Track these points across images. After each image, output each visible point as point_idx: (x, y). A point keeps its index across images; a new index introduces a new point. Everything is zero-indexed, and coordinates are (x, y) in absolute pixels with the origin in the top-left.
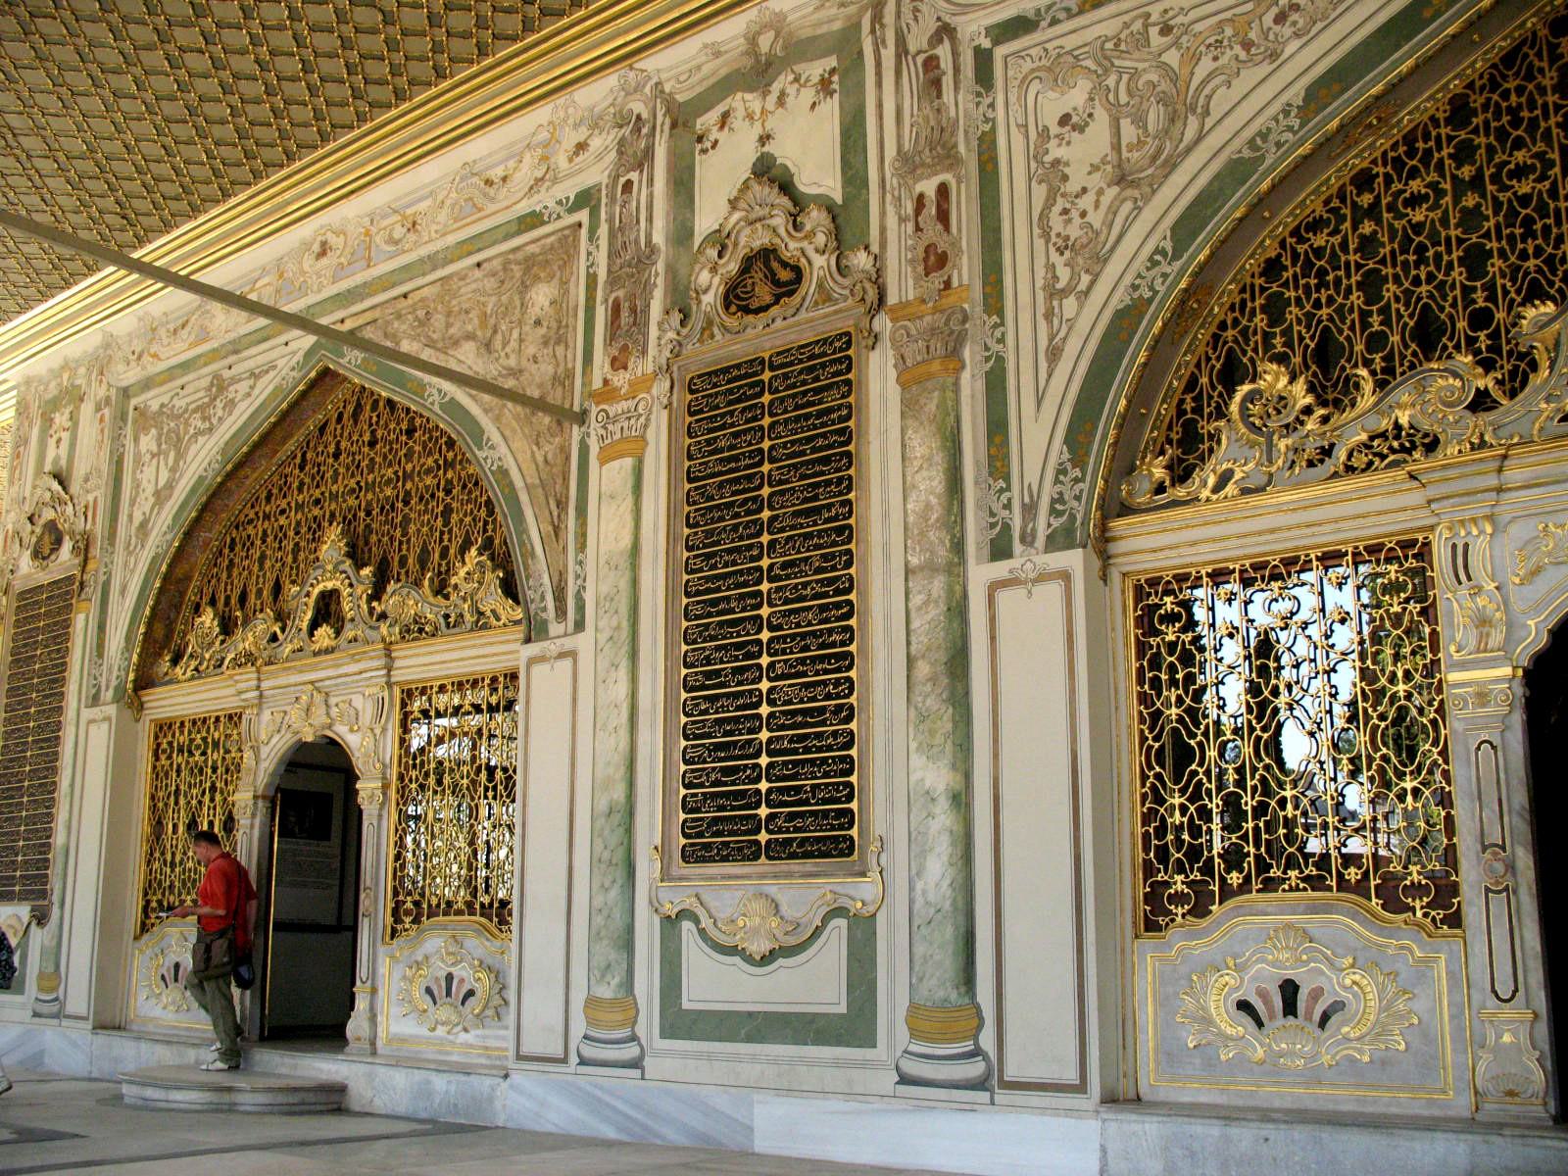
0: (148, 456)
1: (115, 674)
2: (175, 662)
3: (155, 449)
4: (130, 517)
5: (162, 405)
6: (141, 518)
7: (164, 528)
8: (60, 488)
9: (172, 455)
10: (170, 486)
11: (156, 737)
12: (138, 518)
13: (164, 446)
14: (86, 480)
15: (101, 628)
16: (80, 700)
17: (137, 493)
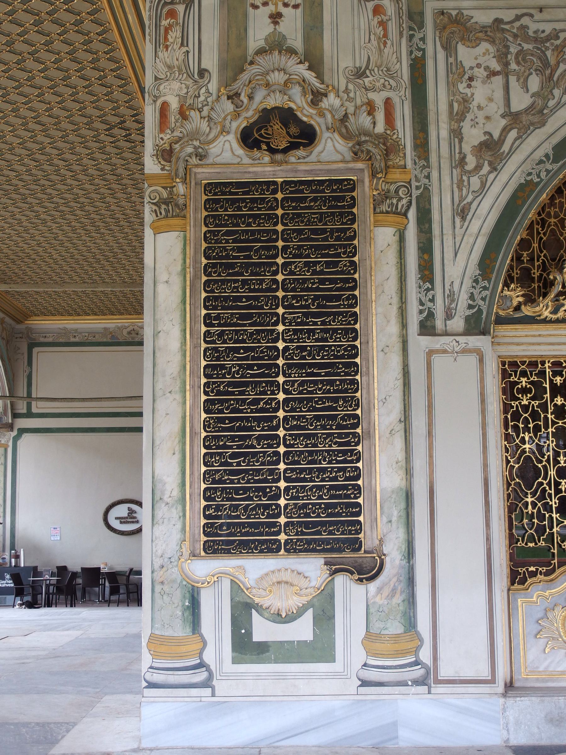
0: (481, 73)
1: (463, 300)
2: (530, 300)
3: (495, 66)
4: (457, 134)
5: (498, 21)
6: (483, 138)
7: (539, 154)
8: (310, 76)
9: (534, 83)
10: (538, 114)
11: (505, 374)
12: (473, 136)
13: (513, 66)
14: (360, 74)
15: (426, 249)
16: (404, 325)
17: (468, 110)
